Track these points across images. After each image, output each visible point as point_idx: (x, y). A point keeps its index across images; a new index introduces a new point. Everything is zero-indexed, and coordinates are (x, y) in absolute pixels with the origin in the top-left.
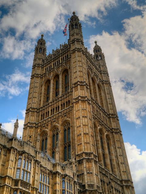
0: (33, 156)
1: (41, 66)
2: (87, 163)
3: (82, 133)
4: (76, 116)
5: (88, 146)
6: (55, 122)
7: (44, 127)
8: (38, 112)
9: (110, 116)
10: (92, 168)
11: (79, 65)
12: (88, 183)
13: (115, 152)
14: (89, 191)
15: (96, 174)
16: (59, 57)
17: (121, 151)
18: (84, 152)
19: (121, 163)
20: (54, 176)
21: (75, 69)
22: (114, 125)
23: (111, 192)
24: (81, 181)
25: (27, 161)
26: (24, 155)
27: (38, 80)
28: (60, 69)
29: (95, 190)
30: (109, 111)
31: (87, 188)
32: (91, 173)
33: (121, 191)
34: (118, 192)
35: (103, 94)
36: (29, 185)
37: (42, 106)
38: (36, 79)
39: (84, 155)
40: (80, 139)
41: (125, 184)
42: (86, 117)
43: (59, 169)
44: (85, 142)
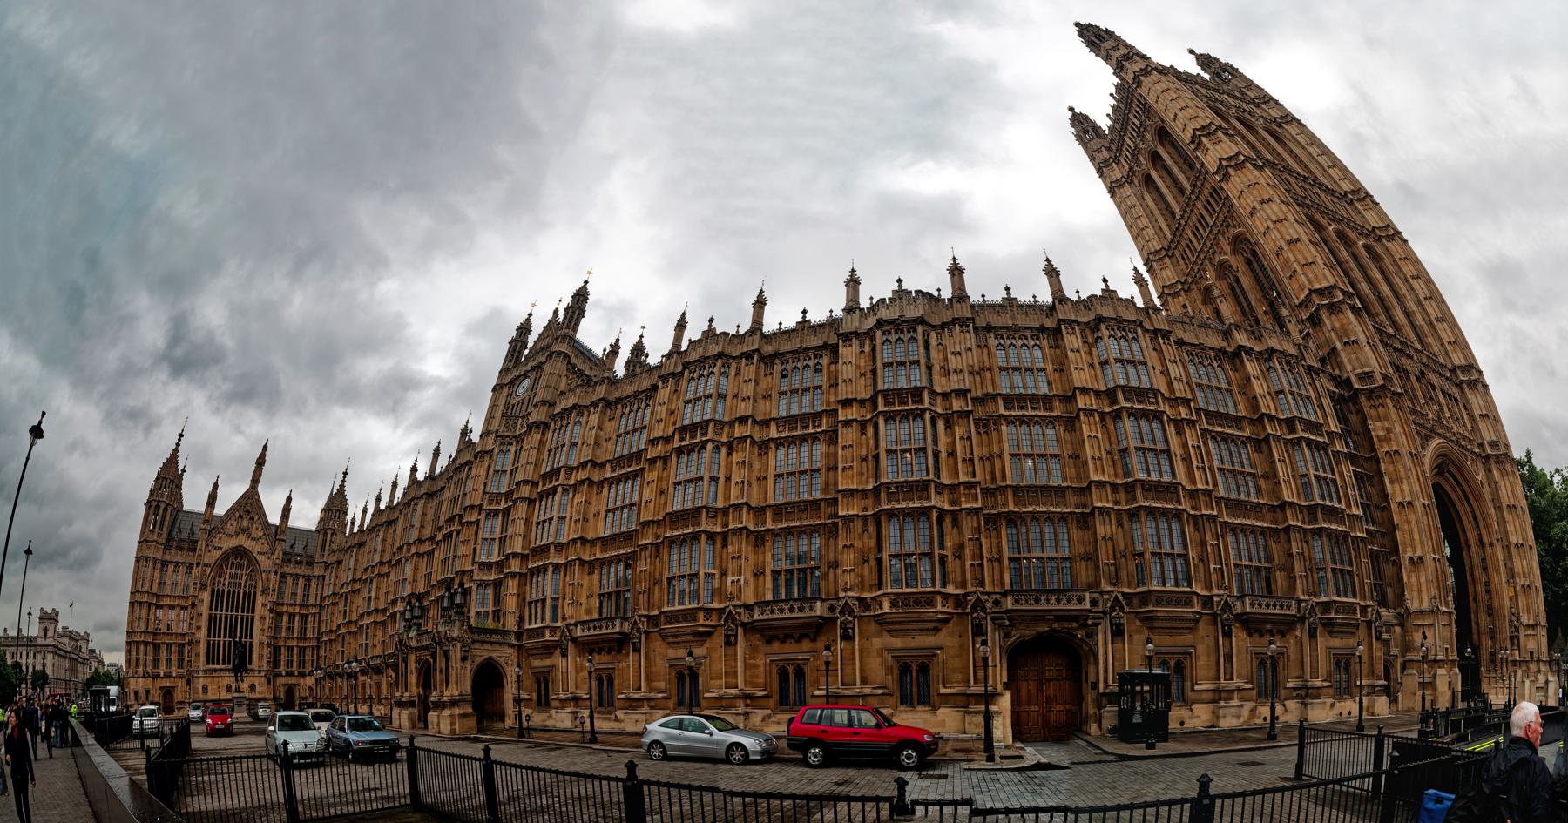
31: (1356, 386)
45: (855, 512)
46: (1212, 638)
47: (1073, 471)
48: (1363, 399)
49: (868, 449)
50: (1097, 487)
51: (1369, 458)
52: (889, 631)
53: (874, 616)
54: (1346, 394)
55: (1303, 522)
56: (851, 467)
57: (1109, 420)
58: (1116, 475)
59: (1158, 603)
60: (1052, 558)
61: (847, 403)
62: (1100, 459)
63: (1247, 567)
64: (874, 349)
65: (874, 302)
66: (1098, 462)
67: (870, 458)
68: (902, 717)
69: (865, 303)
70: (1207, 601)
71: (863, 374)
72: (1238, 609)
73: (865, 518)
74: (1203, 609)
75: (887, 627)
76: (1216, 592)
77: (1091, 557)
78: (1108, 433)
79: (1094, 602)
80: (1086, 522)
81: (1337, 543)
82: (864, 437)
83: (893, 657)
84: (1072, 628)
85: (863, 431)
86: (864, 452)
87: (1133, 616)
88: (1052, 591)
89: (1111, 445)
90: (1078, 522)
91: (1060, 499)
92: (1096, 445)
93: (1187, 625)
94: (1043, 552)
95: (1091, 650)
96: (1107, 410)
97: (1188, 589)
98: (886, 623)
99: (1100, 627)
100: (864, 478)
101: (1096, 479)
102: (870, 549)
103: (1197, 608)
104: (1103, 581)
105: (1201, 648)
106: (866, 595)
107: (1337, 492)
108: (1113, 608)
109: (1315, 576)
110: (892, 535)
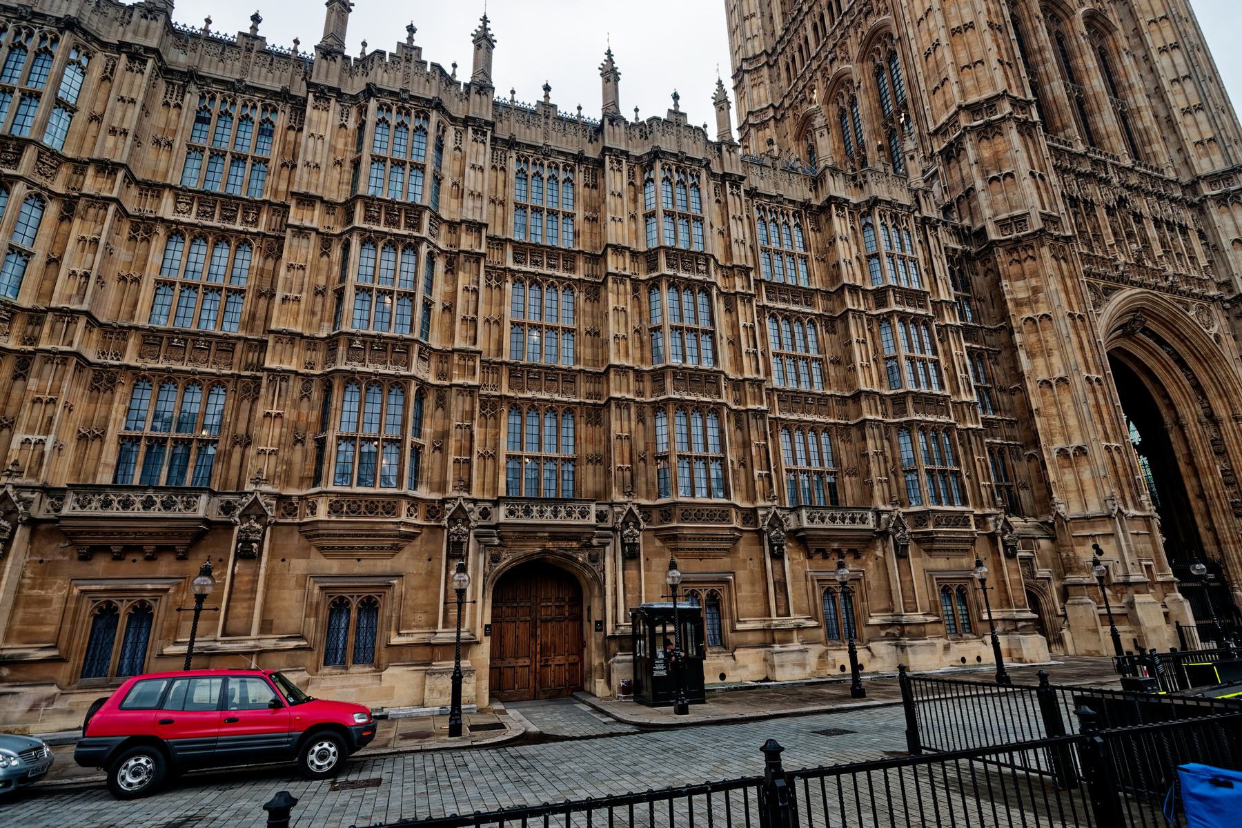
0: (700, 161)
2: (985, 143)
5: (979, 74)
10: (1008, 154)
12: (995, 215)
13: (1150, 77)
15: (1032, 174)
20: (823, 218)
23: (1130, 235)
24: (967, 222)
25: (681, 182)
26: (658, 165)
29: (1034, 234)
32: (1011, 175)
33: (1190, 224)
34: (1171, 229)
36: (707, 261)
39: (964, 121)
43: (836, 187)
44: (964, 61)
45: (293, 367)
46: (756, 562)
47: (589, 351)
48: (1001, 256)
49: (328, 278)
50: (617, 373)
51: (995, 330)
52: (321, 549)
53: (300, 525)
55: (885, 414)
56: (297, 300)
57: (643, 291)
58: (642, 360)
59: (685, 518)
60: (551, 459)
61: (306, 200)
62: (625, 338)
63: (803, 472)
64: (361, 127)
65: (368, 52)
66: (622, 342)
67: (330, 292)
68: (323, 684)
69: (353, 50)
70: (750, 515)
71: (339, 163)
72: (792, 523)
73: (307, 379)
74: (744, 524)
75: (318, 542)
76: (760, 503)
77: (601, 460)
78: (640, 307)
79: (601, 517)
80: (599, 416)
81: (936, 438)
82: (325, 258)
83: (321, 588)
84: (572, 549)
85: (325, 250)
86: (322, 281)
87: (651, 534)
88: (547, 501)
89: (641, 322)
90: (589, 415)
91: (569, 385)
92: (622, 320)
93: (723, 545)
94: (540, 450)
95: (596, 578)
96: (643, 277)
97: (725, 501)
98: (318, 536)
99: (608, 548)
100: (316, 319)
101: (617, 363)
102: (308, 424)
103: (736, 523)
104: (614, 490)
105: (742, 575)
106: (293, 491)
107: (939, 375)
108: (625, 523)
109: (901, 480)
110: (346, 408)
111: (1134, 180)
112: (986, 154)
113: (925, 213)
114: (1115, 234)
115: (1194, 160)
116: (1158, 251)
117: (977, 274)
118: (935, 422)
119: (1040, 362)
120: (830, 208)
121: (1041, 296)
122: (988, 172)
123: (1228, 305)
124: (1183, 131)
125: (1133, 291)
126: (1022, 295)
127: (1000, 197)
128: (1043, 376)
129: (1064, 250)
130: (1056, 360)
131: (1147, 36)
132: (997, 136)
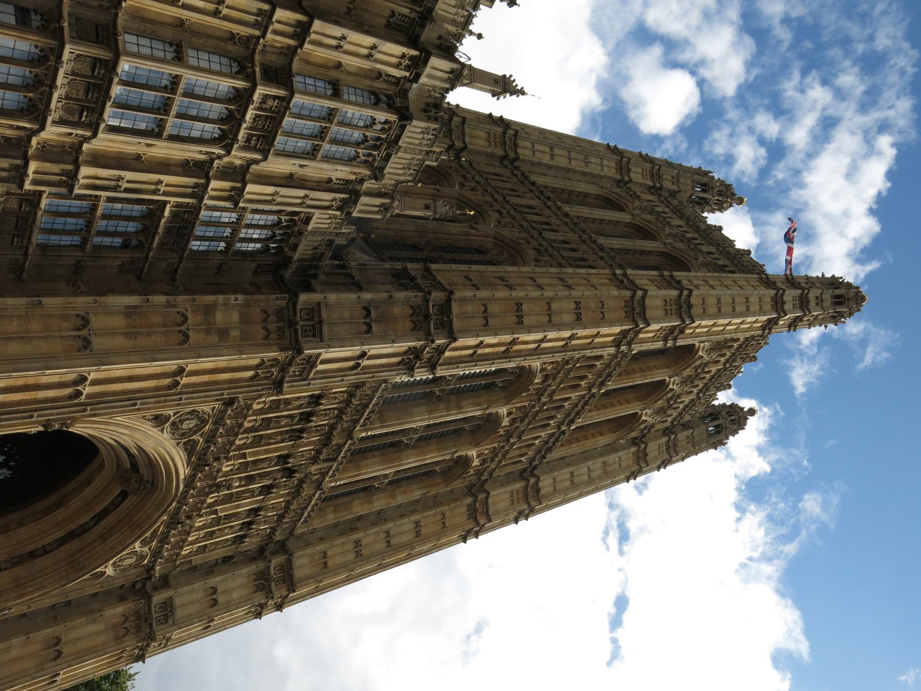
1: (658, 185)
2: (409, 311)
3: (519, 293)
4: (570, 278)
6: (496, 216)
7: (461, 179)
8: (505, 162)
9: (532, 481)
11: (736, 300)
14: (291, 312)
16: (711, 244)
17: (406, 538)
18: (452, 293)
19: (358, 543)
21: (720, 286)
22: (500, 496)
23: (250, 479)
24: (322, 277)
27: (611, 172)
28: (680, 245)
29: (297, 341)
30: (545, 473)
32: (369, 330)
35: (603, 441)
37: (533, 178)
38: (613, 165)
40: (493, 286)
41: (272, 568)
42: (578, 318)
48: (276, 301)
54: (288, 274)
111: (306, 491)
112: (397, 310)
113: (364, 200)
114: (255, 462)
115: (309, 551)
116: (223, 510)
117: (255, 273)
118: (53, 86)
119: (119, 322)
120: (416, 48)
121: (215, 338)
122: (377, 308)
123: (139, 586)
124: (341, 541)
125: (182, 477)
126: (219, 317)
127: (346, 314)
128: (96, 322)
129: (266, 378)
130: (119, 342)
131: (433, 512)
132: (412, 325)
